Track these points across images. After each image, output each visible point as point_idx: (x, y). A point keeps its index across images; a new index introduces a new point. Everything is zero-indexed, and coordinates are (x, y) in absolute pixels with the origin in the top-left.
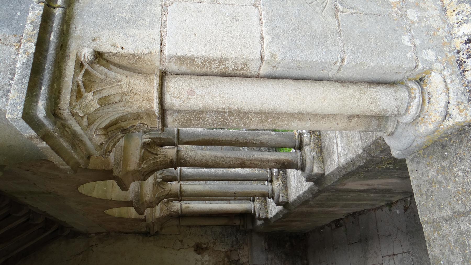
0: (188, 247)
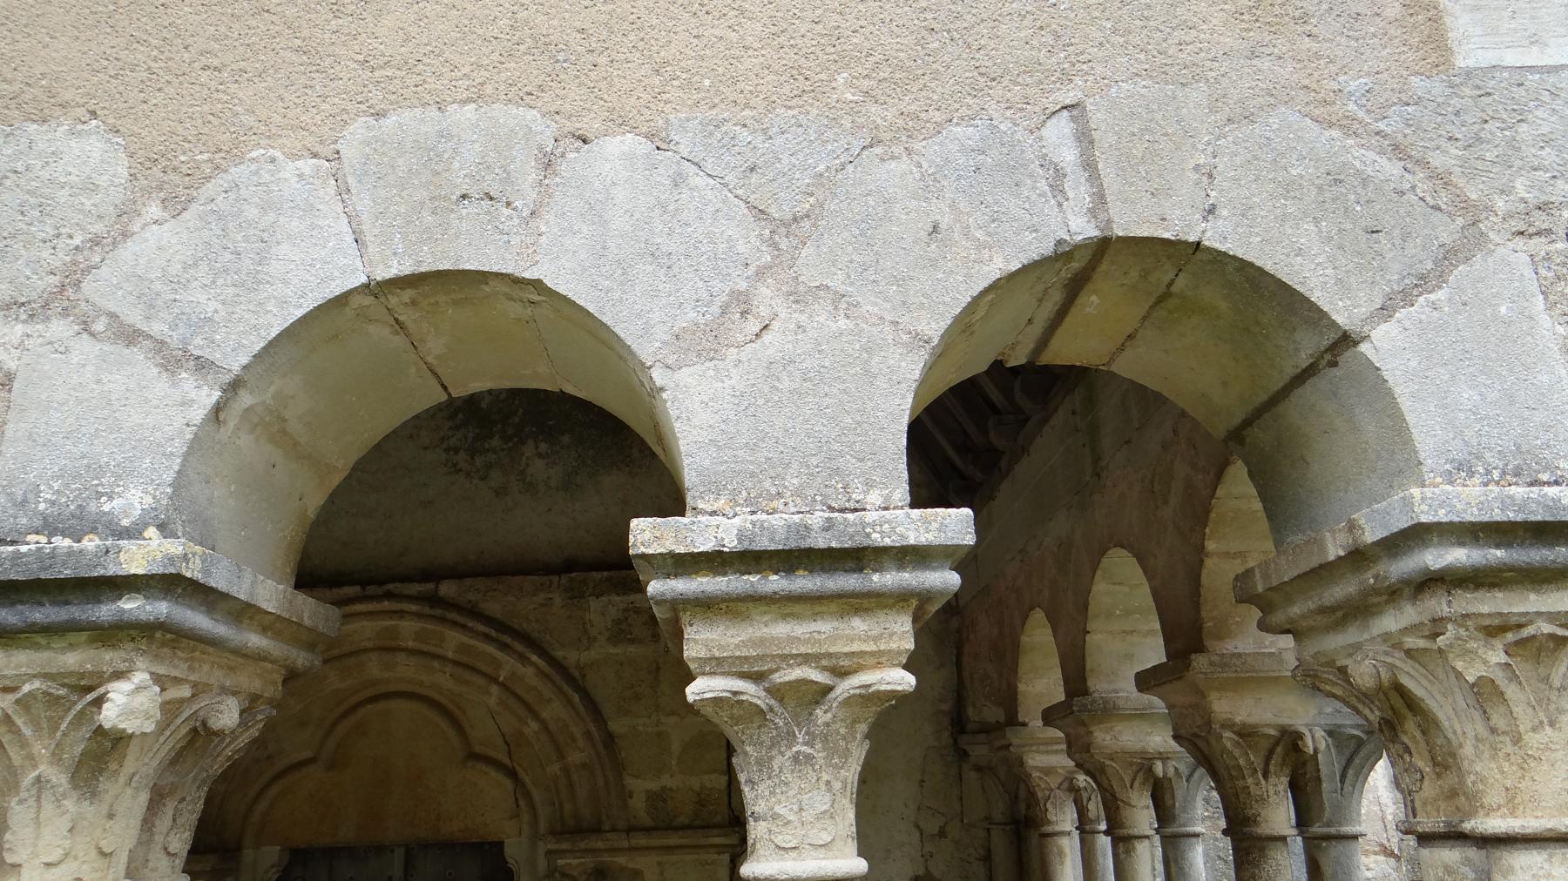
0: (927, 857)
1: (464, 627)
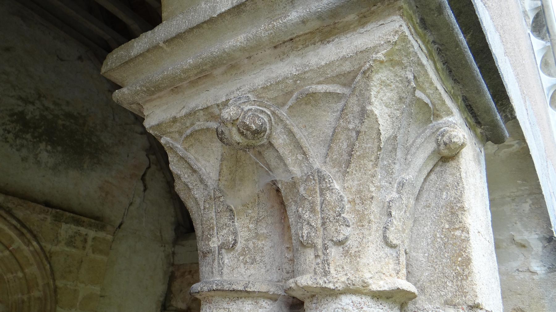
1: (5, 219)
